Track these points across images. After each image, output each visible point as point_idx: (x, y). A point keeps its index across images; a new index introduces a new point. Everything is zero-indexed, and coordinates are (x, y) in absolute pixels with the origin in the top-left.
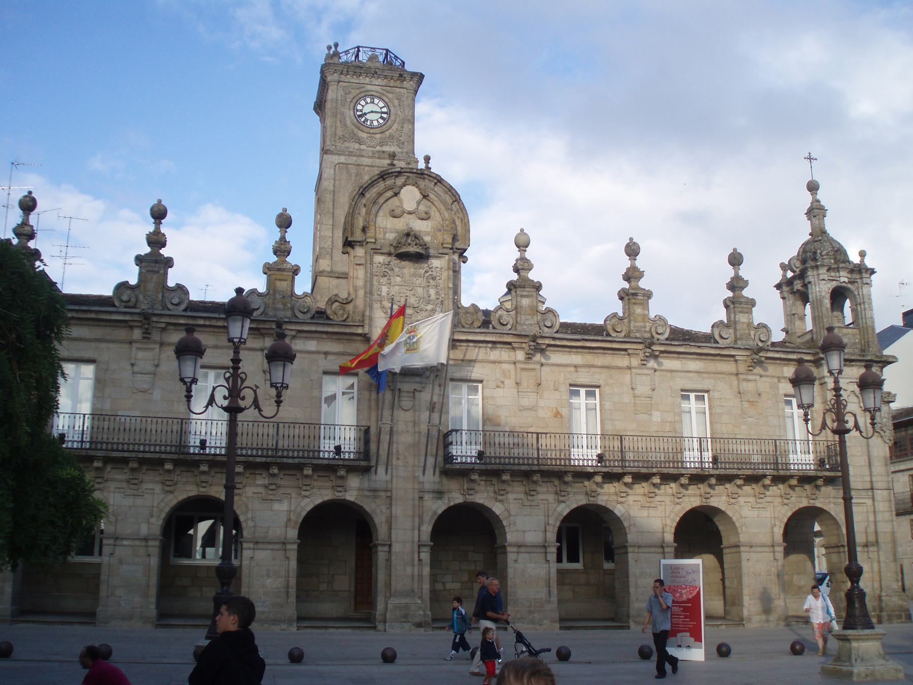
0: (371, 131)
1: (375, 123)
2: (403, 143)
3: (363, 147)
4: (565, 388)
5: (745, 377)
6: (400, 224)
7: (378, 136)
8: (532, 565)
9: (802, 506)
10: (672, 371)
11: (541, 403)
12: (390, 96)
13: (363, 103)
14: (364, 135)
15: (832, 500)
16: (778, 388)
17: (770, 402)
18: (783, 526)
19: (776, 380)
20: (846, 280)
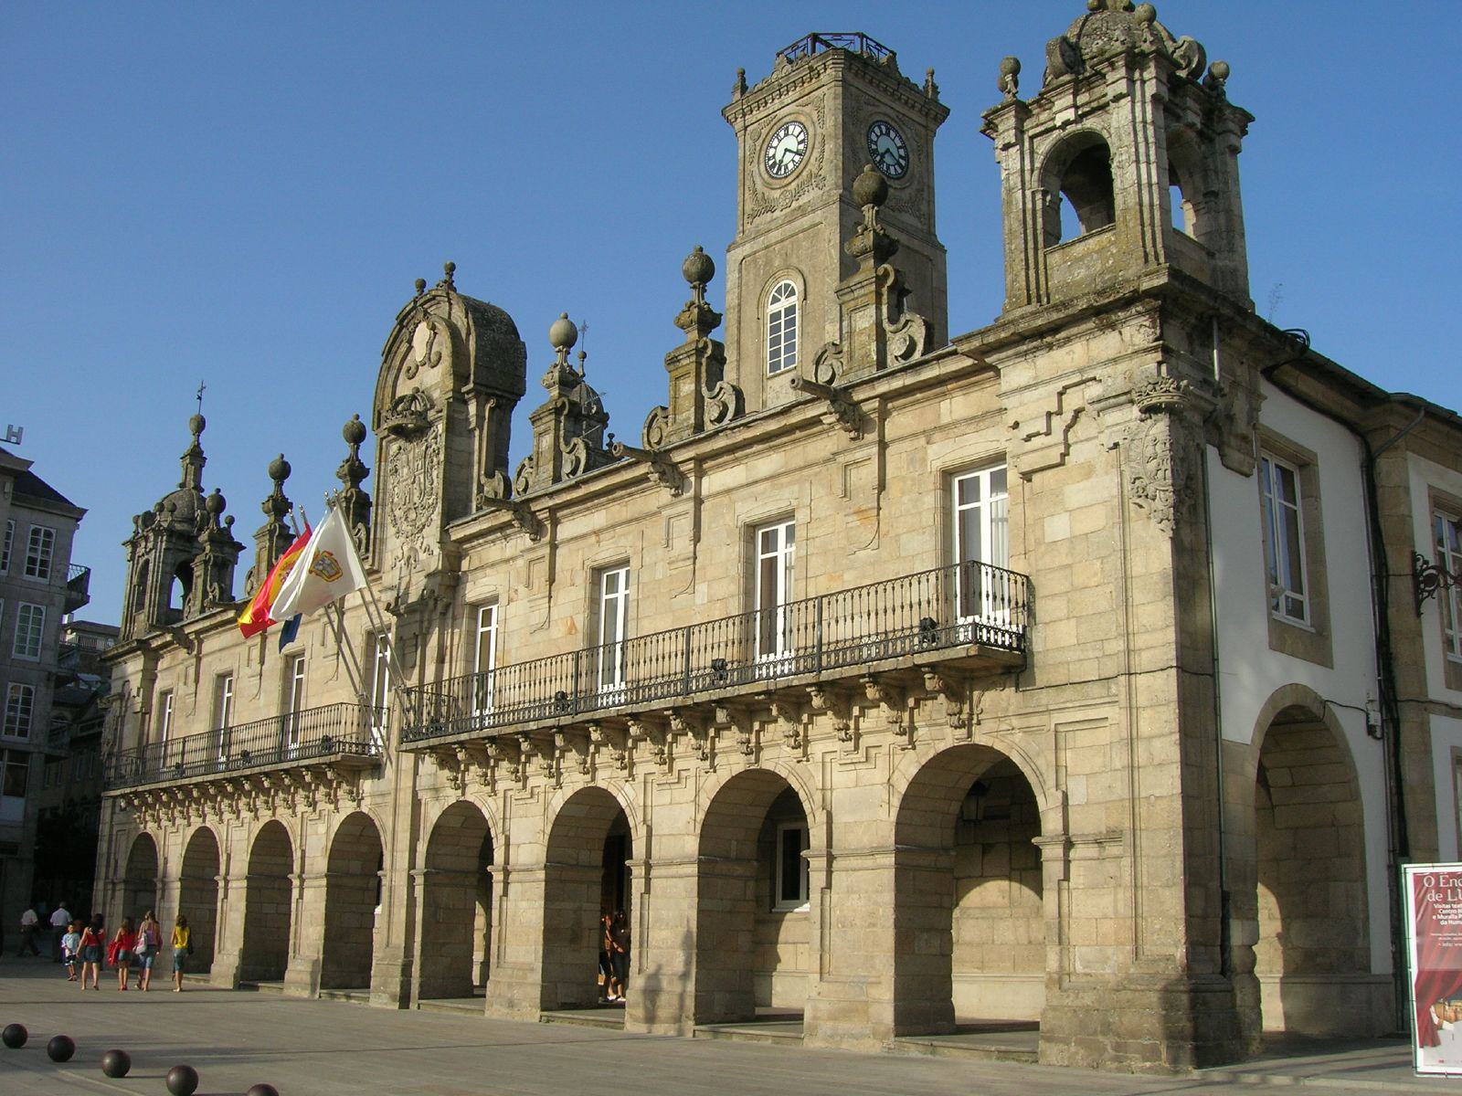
0: (786, 181)
1: (791, 166)
2: (824, 178)
3: (777, 213)
4: (582, 578)
5: (849, 457)
6: (415, 383)
7: (794, 185)
8: (524, 904)
9: (942, 747)
10: (728, 491)
11: (554, 616)
12: (807, 109)
13: (775, 143)
14: (779, 192)
15: (1015, 722)
16: (924, 460)
17: (905, 499)
18: (896, 802)
19: (922, 440)
20: (1070, 114)
